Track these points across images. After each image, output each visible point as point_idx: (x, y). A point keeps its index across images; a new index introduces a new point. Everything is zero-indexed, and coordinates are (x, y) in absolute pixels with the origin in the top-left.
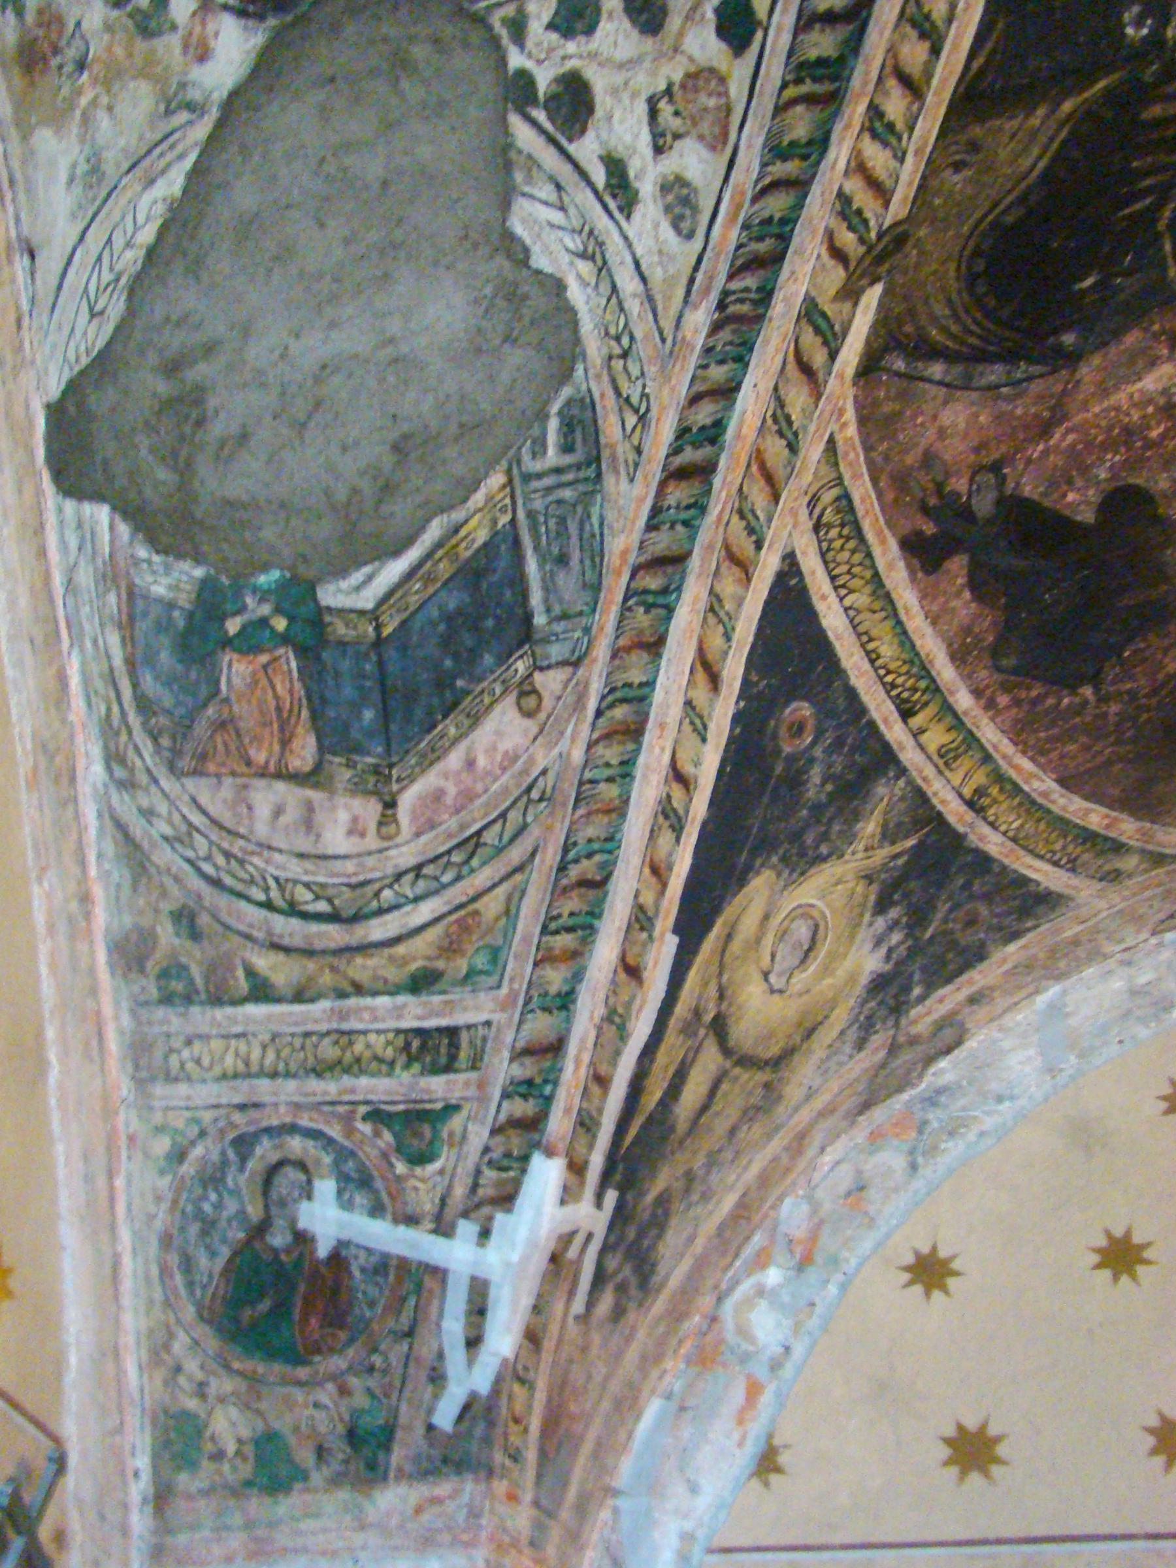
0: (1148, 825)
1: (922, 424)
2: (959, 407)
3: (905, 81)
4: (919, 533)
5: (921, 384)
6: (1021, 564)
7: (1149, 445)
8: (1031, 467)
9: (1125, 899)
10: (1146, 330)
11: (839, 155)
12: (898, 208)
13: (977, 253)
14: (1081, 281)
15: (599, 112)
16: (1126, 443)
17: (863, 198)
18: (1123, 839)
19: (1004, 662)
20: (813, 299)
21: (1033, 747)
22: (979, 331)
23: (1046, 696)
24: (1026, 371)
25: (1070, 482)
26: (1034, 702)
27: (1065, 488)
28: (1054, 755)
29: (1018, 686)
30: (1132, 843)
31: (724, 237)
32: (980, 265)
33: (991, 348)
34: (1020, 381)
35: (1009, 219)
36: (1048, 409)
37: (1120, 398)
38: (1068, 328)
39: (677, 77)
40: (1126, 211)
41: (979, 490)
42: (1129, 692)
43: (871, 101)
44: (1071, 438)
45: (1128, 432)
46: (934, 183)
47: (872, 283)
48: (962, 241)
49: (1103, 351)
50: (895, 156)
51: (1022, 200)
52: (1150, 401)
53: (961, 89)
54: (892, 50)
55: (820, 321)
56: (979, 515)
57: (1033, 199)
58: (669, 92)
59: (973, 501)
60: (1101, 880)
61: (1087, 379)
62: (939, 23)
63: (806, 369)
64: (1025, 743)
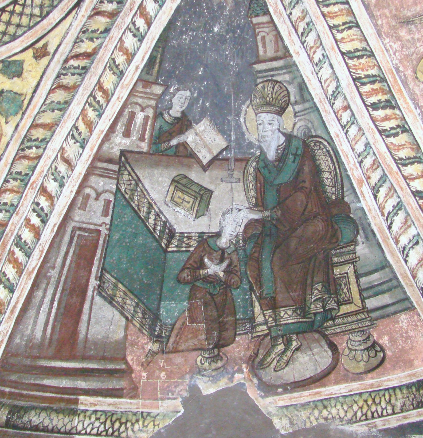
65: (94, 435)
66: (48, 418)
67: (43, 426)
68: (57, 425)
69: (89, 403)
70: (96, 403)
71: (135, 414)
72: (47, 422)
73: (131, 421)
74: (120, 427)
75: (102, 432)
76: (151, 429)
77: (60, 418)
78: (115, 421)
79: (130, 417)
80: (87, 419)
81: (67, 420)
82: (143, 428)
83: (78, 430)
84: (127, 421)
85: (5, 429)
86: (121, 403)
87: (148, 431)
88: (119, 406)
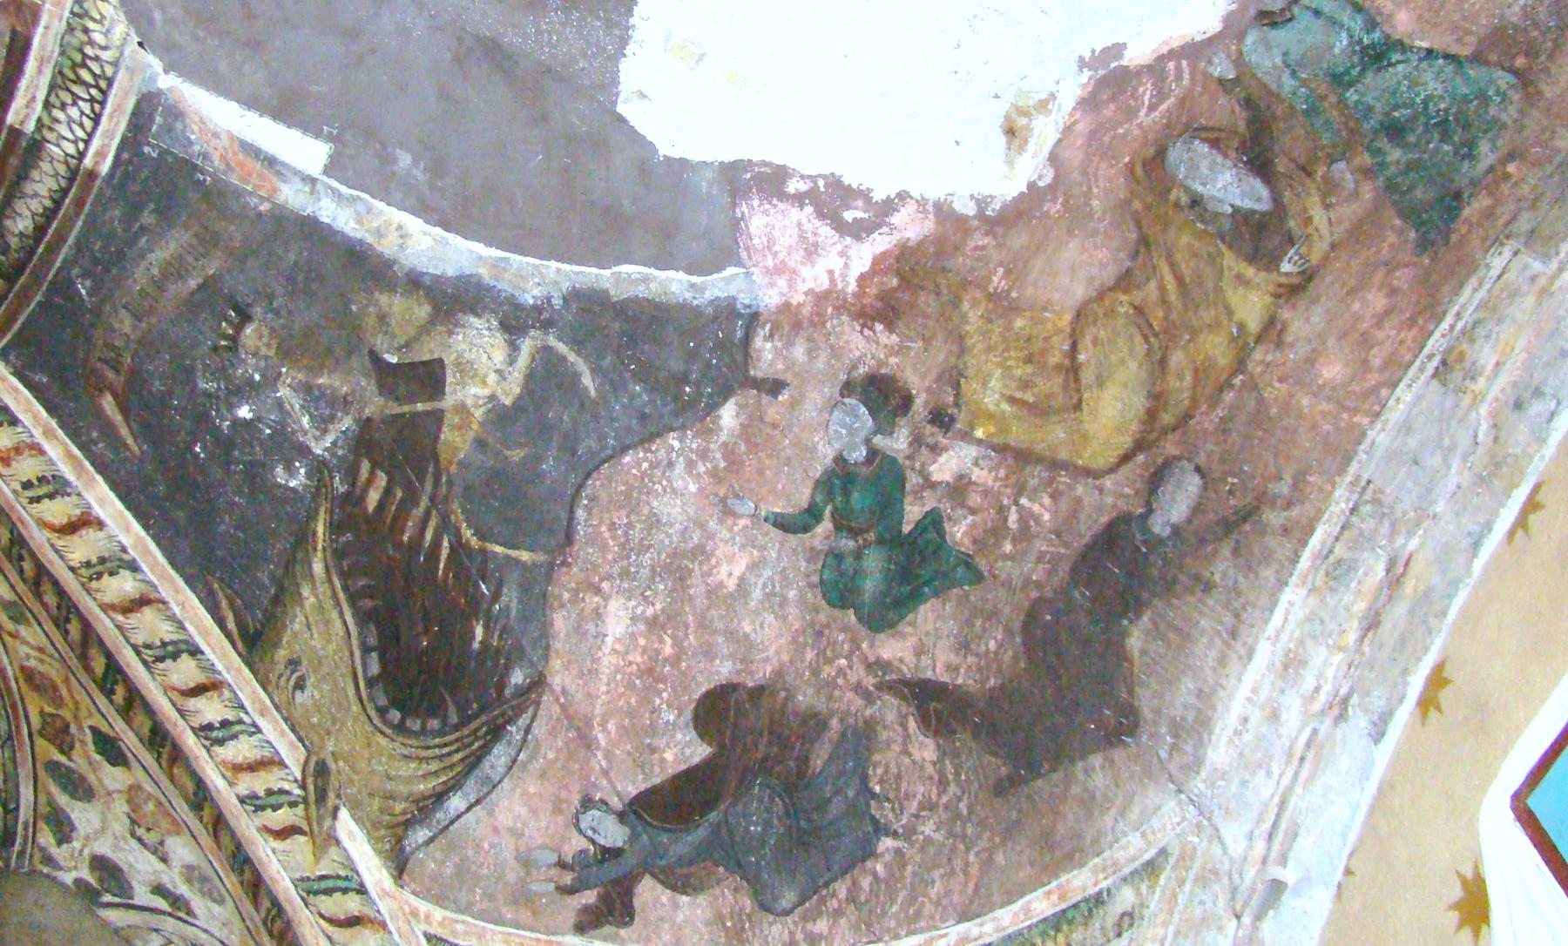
0: (1096, 860)
1: (492, 846)
2: (505, 803)
3: (198, 690)
4: (586, 909)
5: (456, 825)
6: (699, 834)
7: (675, 661)
8: (612, 774)
9: (1165, 924)
10: (562, 606)
11: (215, 780)
12: (293, 756)
13: (382, 712)
14: (473, 638)
15: (125, 868)
16: (658, 681)
17: (258, 783)
18: (1092, 891)
19: (785, 903)
20: (302, 879)
21: (899, 924)
22: (453, 748)
23: (855, 883)
24: (518, 731)
25: (653, 750)
26: (852, 899)
27: (656, 755)
28: (928, 908)
29: (823, 901)
30: (1104, 885)
31: (233, 884)
32: (395, 715)
33: (476, 745)
34: (524, 740)
35: (375, 669)
36: (568, 730)
37: (607, 661)
38: (508, 669)
39: (126, 808)
40: (442, 566)
41: (594, 831)
42: (922, 807)
43: (192, 728)
44: (611, 726)
45: (648, 672)
46: (297, 714)
47: (335, 817)
48: (363, 718)
49: (553, 655)
50: (252, 734)
51: (366, 650)
52: (633, 637)
53: (240, 645)
54: (167, 689)
55: (324, 885)
56: (620, 844)
57: (372, 641)
58: (134, 822)
59: (602, 842)
60: (1119, 935)
61: (567, 682)
62: (175, 637)
63: (353, 922)
64: (888, 930)
65: (94, 129)
66: (28, 200)
67: (42, 215)
68: (50, 190)
69: (25, 111)
70: (29, 96)
71: (71, 29)
72: (35, 205)
73: (83, 43)
74: (90, 70)
75: (93, 111)
76: (112, 10)
77: (38, 178)
78: (78, 77)
79: (75, 42)
80: (57, 126)
81: (45, 166)
82: (103, 25)
83: (76, 155)
84: (81, 50)
85: (17, 287)
86: (43, 47)
87: (112, 19)
88: (47, 54)
